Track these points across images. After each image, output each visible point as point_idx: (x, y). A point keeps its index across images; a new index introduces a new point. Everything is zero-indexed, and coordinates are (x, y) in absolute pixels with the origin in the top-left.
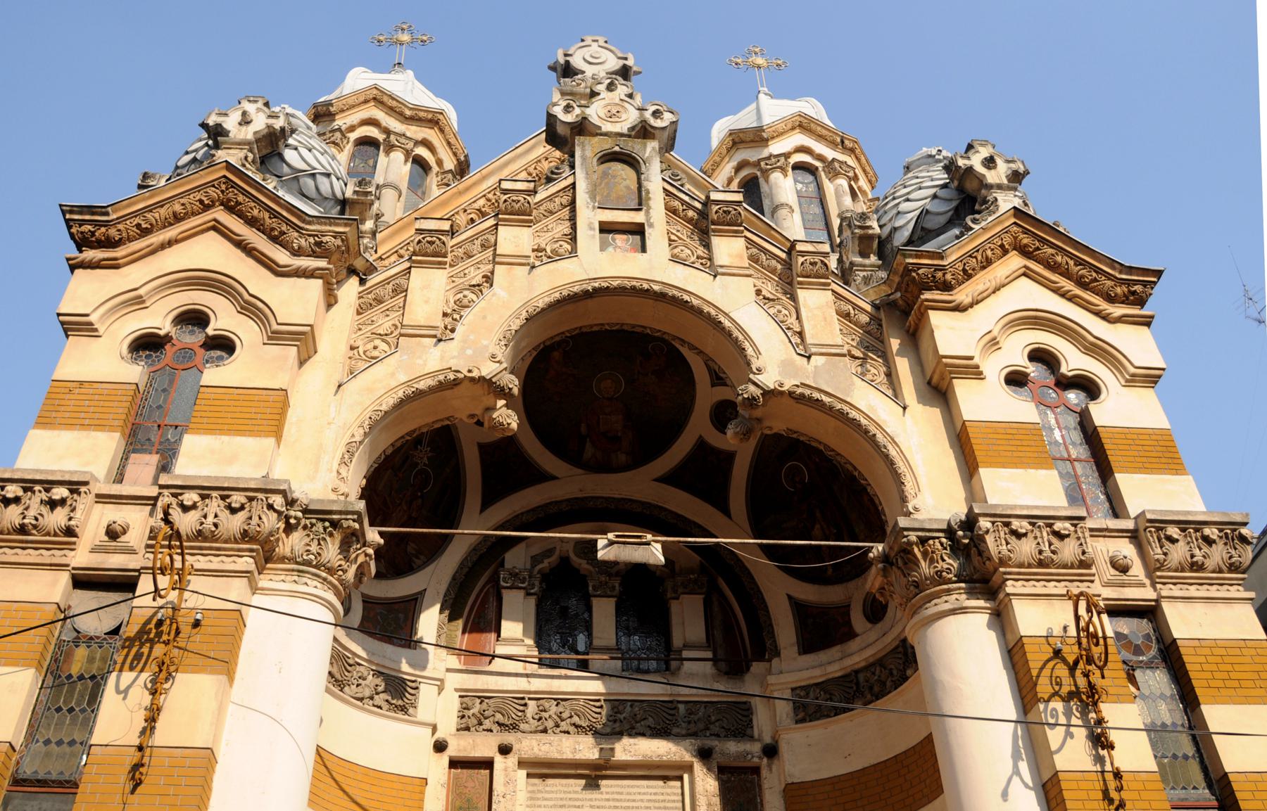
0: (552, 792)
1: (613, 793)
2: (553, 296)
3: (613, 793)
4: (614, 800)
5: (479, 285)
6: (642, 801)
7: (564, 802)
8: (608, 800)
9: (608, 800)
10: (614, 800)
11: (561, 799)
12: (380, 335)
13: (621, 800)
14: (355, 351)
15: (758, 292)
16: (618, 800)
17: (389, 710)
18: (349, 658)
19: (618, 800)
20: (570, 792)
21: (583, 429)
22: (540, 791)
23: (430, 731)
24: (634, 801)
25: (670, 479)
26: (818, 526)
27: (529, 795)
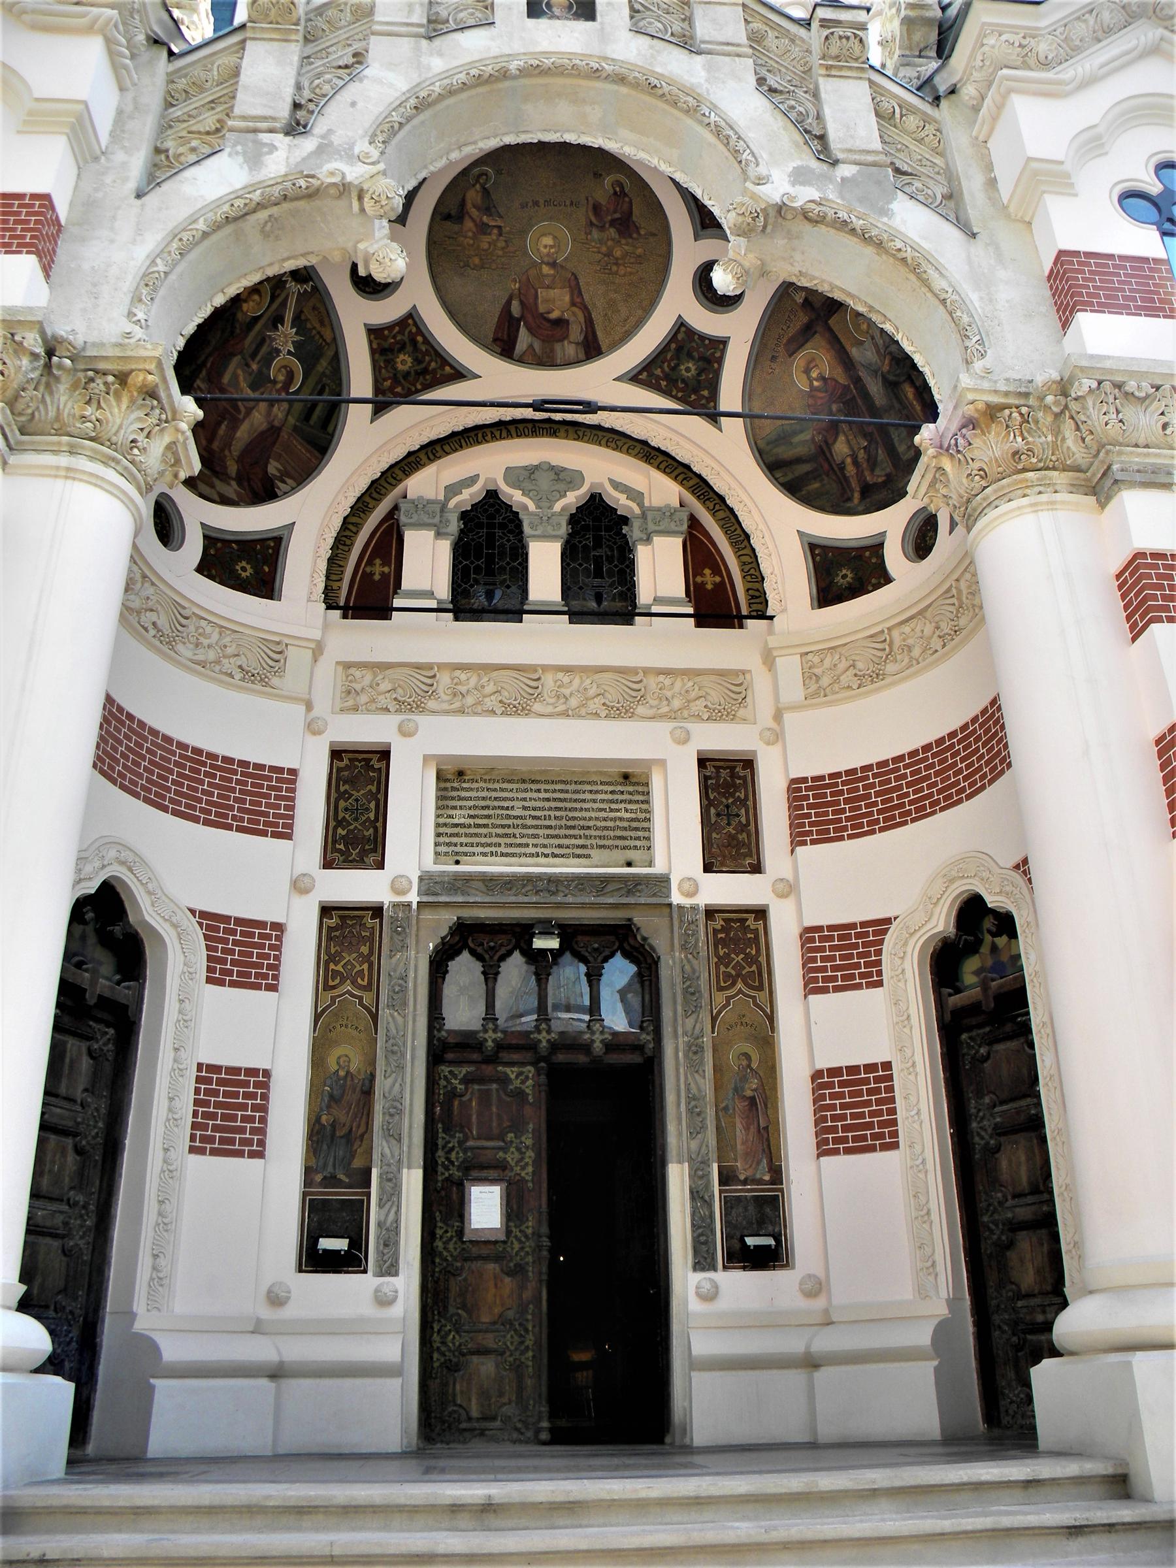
0: (472, 789)
1: (554, 791)
2: (457, 77)
3: (554, 791)
4: (555, 800)
5: (347, 67)
6: (594, 801)
7: (488, 803)
8: (548, 800)
9: (548, 800)
10: (555, 800)
11: (484, 799)
12: (199, 133)
13: (565, 800)
14: (163, 157)
15: (761, 81)
16: (560, 800)
17: (243, 679)
18: (184, 608)
19: (560, 800)
20: (495, 790)
21: (515, 304)
22: (454, 789)
23: (302, 708)
24: (584, 801)
25: (643, 376)
26: (842, 438)
27: (440, 793)
